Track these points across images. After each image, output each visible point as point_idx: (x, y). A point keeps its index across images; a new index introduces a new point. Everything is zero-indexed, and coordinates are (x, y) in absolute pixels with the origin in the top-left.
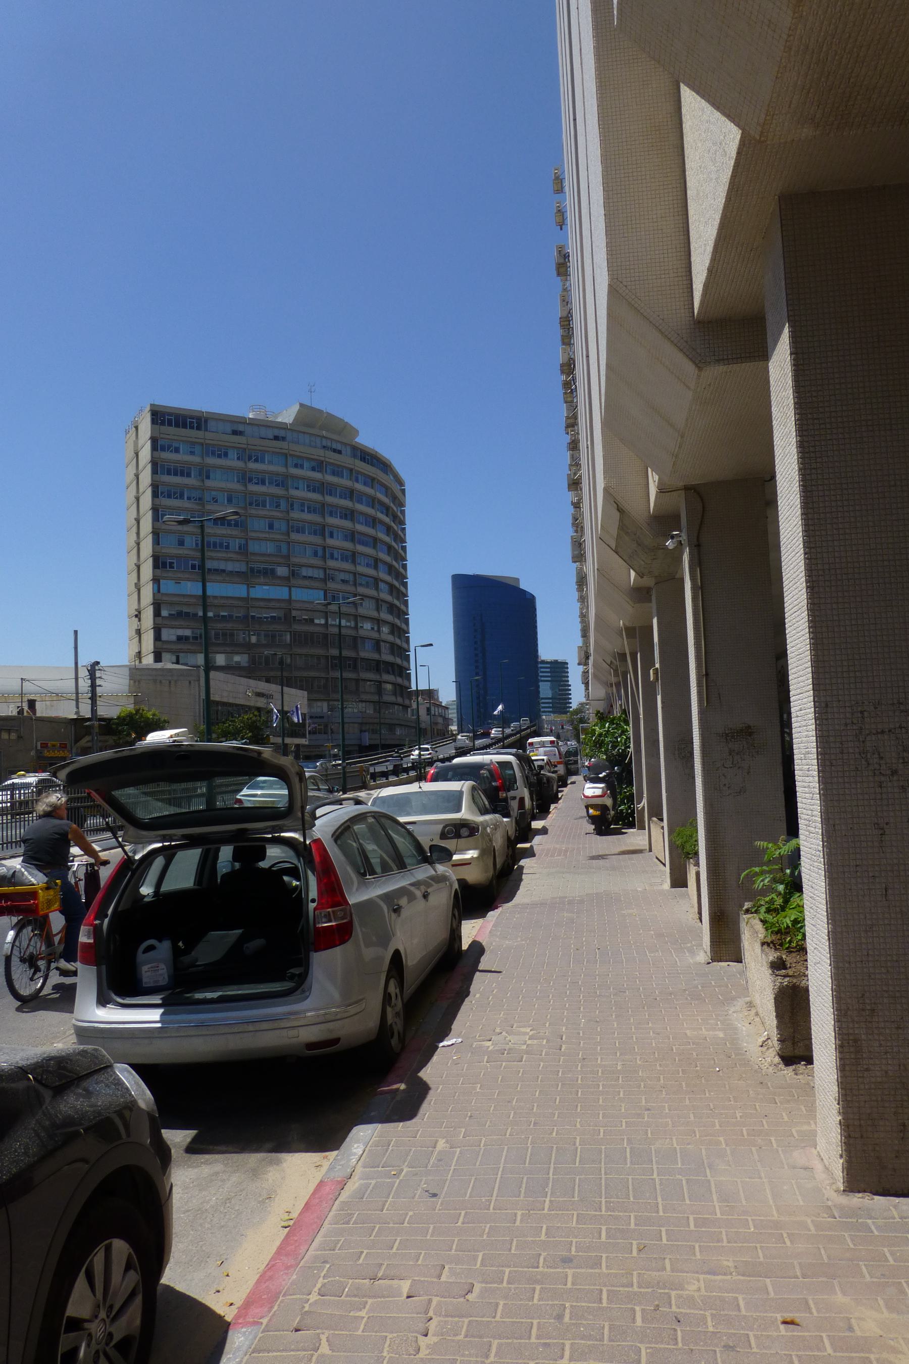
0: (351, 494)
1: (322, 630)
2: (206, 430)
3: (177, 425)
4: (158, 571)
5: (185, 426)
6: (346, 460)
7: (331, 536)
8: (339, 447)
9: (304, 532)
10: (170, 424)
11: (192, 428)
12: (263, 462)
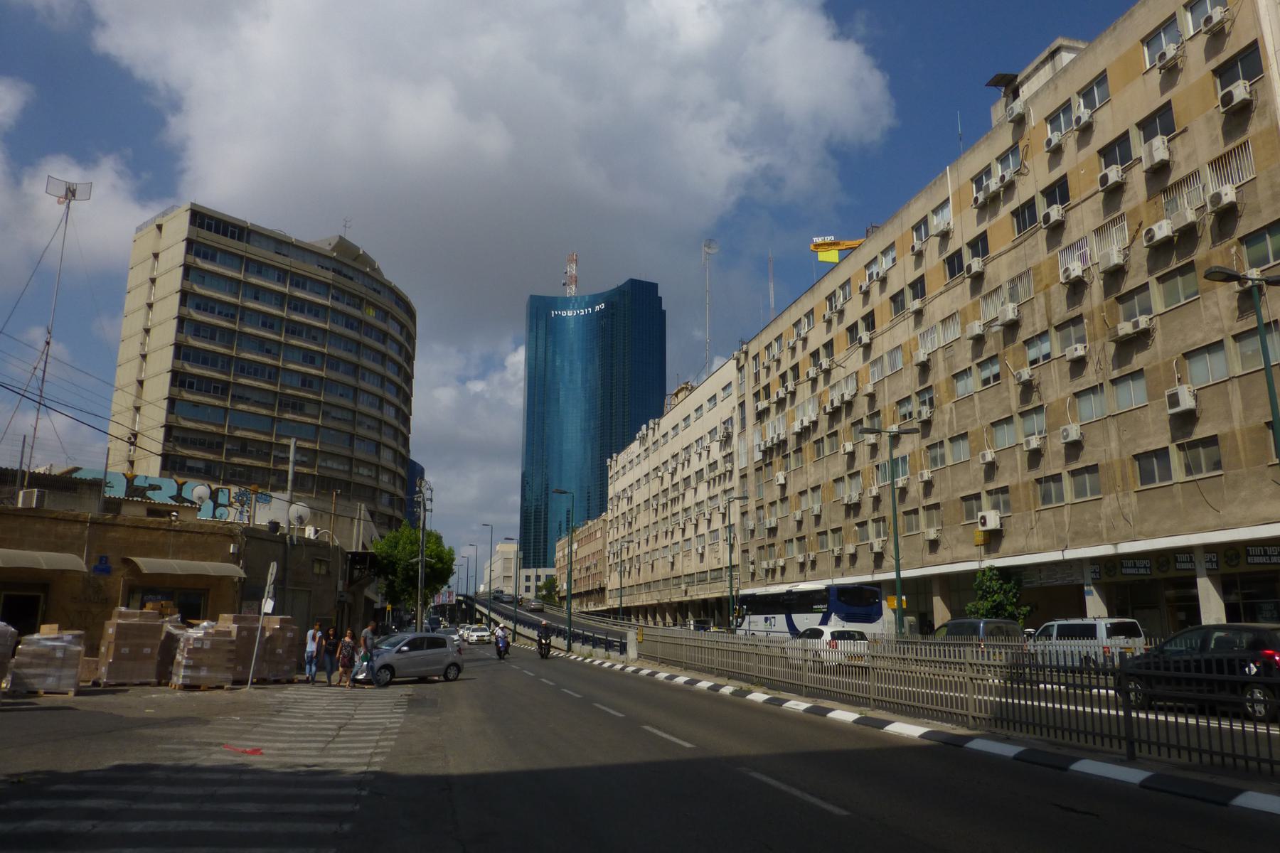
1: (344, 477)
2: (248, 242)
3: (217, 232)
4: (176, 390)
5: (225, 234)
6: (385, 301)
8: (379, 288)
9: (337, 370)
10: (209, 229)
11: (232, 237)
12: (304, 288)
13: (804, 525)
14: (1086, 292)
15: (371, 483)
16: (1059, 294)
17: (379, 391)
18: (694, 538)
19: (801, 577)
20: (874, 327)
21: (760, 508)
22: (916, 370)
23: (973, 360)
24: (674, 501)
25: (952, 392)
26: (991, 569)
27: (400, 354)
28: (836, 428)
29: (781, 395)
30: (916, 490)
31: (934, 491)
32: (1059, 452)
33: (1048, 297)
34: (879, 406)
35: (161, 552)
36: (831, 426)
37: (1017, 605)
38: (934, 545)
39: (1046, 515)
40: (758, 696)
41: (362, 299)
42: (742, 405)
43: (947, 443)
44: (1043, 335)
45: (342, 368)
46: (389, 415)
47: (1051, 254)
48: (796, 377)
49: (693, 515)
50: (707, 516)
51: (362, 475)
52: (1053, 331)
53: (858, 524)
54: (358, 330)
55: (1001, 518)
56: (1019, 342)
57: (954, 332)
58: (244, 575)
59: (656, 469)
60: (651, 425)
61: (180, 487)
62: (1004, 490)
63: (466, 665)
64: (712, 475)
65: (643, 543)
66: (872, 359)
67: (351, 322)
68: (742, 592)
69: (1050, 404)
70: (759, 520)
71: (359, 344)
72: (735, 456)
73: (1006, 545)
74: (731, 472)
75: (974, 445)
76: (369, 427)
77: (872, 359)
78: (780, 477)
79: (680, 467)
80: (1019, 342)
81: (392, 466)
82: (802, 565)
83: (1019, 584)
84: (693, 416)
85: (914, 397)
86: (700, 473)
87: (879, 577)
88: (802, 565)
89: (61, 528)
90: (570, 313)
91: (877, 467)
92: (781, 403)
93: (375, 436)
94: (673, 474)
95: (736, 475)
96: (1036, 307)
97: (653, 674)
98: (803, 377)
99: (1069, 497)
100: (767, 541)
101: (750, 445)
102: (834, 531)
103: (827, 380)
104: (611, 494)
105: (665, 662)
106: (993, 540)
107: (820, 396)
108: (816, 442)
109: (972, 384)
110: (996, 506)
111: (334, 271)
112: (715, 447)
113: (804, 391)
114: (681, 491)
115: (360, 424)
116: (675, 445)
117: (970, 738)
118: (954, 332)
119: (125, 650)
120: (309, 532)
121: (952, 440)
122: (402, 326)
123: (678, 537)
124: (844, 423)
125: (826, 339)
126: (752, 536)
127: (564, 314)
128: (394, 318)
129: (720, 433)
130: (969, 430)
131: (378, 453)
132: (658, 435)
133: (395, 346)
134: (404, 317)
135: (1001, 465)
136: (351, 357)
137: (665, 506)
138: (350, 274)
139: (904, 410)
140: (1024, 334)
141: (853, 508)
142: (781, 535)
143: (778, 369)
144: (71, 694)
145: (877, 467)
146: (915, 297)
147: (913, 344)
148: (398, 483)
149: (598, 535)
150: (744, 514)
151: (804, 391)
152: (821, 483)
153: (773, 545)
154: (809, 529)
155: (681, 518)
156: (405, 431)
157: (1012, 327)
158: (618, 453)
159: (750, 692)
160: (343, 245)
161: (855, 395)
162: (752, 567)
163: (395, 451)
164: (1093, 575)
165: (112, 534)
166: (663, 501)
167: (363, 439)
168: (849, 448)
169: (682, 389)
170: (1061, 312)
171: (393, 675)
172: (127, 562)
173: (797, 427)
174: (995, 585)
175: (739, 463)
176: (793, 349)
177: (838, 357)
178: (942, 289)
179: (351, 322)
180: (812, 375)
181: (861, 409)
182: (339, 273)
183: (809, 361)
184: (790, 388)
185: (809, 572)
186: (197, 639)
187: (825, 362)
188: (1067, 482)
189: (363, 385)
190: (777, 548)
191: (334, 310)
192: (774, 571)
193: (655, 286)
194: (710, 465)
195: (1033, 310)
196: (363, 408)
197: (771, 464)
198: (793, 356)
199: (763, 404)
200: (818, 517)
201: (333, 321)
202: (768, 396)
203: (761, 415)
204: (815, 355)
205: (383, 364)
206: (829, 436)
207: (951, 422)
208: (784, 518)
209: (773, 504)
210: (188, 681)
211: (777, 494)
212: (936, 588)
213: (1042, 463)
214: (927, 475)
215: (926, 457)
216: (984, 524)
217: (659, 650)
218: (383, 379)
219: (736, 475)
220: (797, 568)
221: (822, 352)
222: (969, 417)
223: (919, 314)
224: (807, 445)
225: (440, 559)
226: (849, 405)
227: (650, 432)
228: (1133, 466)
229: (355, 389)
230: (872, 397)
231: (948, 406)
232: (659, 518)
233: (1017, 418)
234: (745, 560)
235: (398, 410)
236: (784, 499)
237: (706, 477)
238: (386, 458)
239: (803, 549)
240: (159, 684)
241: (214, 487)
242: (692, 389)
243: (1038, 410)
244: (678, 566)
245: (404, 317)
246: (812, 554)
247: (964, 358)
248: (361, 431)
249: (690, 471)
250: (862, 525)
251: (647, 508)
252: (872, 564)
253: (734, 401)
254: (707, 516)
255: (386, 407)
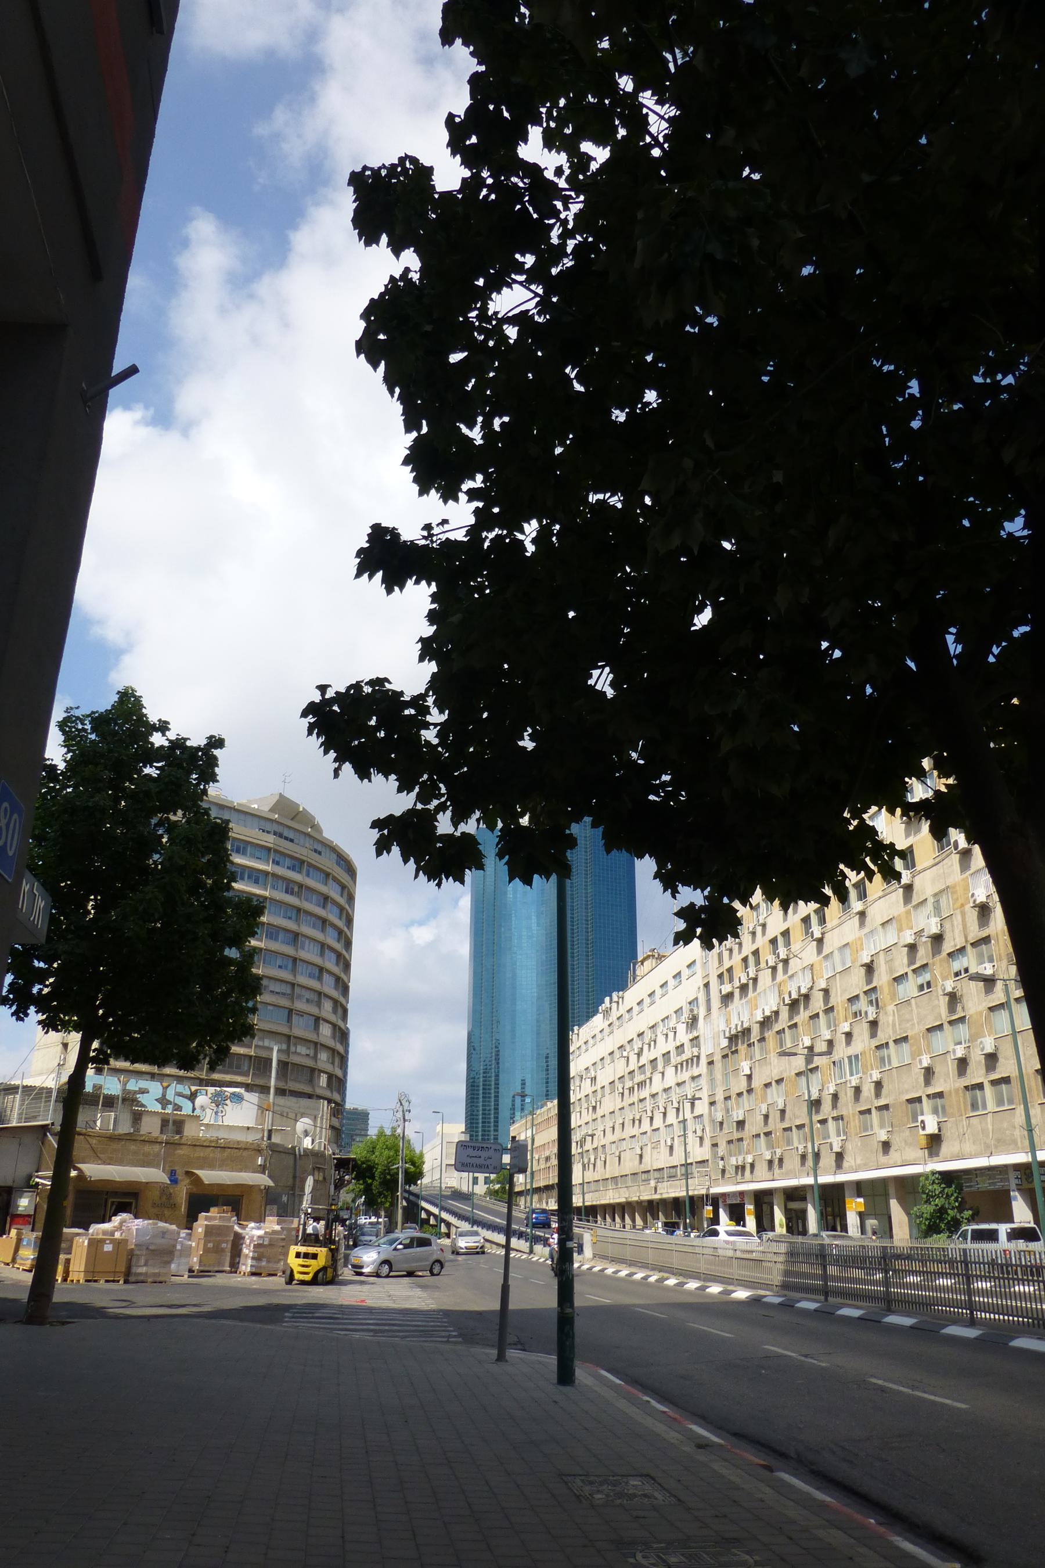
0: (326, 899)
6: (327, 862)
7: (303, 948)
8: (319, 848)
9: (276, 940)
12: (244, 853)
13: (770, 1120)
14: (992, 915)
15: (310, 1063)
16: (973, 915)
17: (318, 960)
18: (662, 1129)
19: (769, 1176)
20: (825, 922)
21: (727, 1098)
22: (863, 970)
23: (909, 966)
24: (641, 1085)
25: (894, 995)
26: (933, 1173)
27: (340, 919)
28: (796, 1020)
29: (744, 981)
30: (868, 1090)
31: (884, 1091)
32: (980, 1062)
33: (963, 914)
34: (833, 1002)
35: (223, 1165)
36: (791, 1018)
37: (961, 1209)
38: (886, 1146)
39: (975, 1121)
40: (672, 1282)
41: (302, 862)
42: (707, 985)
43: (891, 1044)
44: (962, 950)
45: (281, 936)
46: (328, 986)
47: (964, 876)
48: (758, 962)
49: (661, 1100)
50: (676, 1105)
51: (299, 1054)
52: (969, 947)
53: (820, 1122)
54: (298, 895)
55: (939, 1123)
56: (944, 954)
57: (889, 938)
58: (271, 1184)
59: (621, 1047)
60: (615, 998)
61: (165, 1088)
62: (940, 1095)
63: (447, 1264)
64: (679, 1059)
65: (609, 1131)
66: (824, 954)
67: (291, 887)
68: (713, 1191)
69: (971, 1016)
70: (728, 1111)
71: (299, 910)
72: (702, 1039)
73: (945, 1149)
74: (698, 1057)
75: (914, 1049)
76: (308, 1001)
77: (824, 954)
78: (745, 1067)
79: (646, 1047)
80: (944, 954)
81: (331, 1043)
82: (770, 1162)
83: (960, 1188)
84: (659, 992)
85: (862, 996)
86: (666, 1055)
87: (841, 1178)
88: (770, 1162)
89: (147, 1148)
91: (834, 1063)
92: (744, 988)
93: (313, 1010)
94: (639, 1055)
95: (703, 1061)
96: (955, 923)
97: (603, 1270)
98: (763, 965)
99: (991, 1106)
100: (736, 1135)
101: (716, 1030)
102: (800, 1127)
103: (785, 970)
104: (573, 1072)
105: (614, 1260)
106: (934, 1142)
107: (780, 985)
108: (778, 1032)
109: (909, 988)
110: (935, 1111)
111: (275, 834)
112: (682, 1028)
113: (765, 977)
114: (648, 1075)
115: (300, 997)
116: (640, 1023)
117: (765, 1296)
118: (889, 938)
119: (210, 1245)
120: (307, 1143)
121: (895, 1041)
122: (343, 887)
123: (646, 1126)
124: (802, 1016)
125: (783, 928)
126: (721, 1129)
128: (335, 879)
129: (685, 1015)
130: (910, 1033)
131: (316, 1027)
132: (623, 1009)
133: (336, 910)
134: (344, 877)
135: (936, 1070)
136: (291, 925)
137: (631, 1090)
138: (291, 835)
139: (855, 1008)
140: (948, 947)
141: (815, 1104)
142: (750, 1129)
143: (740, 952)
144: (186, 1276)
145: (834, 1063)
146: (860, 898)
147: (859, 943)
148: (337, 1061)
150: (712, 1104)
151: (765, 977)
152: (784, 1076)
153: (741, 1140)
154: (775, 1124)
155: (648, 1104)
156: (344, 1002)
157: (938, 939)
158: (580, 1026)
159: (667, 1279)
160: (283, 805)
161: (811, 988)
162: (721, 1163)
163: (334, 1026)
164: (1017, 1181)
165: (179, 1152)
166: (629, 1084)
167: (301, 1014)
168: (807, 1042)
169: (648, 957)
170: (975, 932)
171: (391, 1270)
172: (189, 1174)
173: (759, 1018)
174: (937, 1189)
175: (707, 1048)
176: (754, 934)
177: (795, 947)
178: (881, 894)
179: (291, 887)
180: (771, 963)
181: (817, 1003)
182: (281, 836)
183: (768, 948)
184: (752, 975)
185: (777, 1171)
186: (259, 1237)
187: (783, 953)
188: (988, 1089)
189: (303, 954)
190: (745, 1143)
191: (274, 875)
192: (743, 1167)
194: (677, 1048)
195: (953, 926)
196: (302, 980)
197: (736, 1051)
198: (753, 941)
199: (727, 988)
200: (783, 1112)
201: (273, 887)
202: (731, 980)
203: (727, 998)
204: (774, 941)
205: (323, 931)
206: (790, 1027)
207: (894, 1025)
208: (751, 1110)
209: (740, 1095)
210: (254, 1270)
211: (743, 1085)
212: (892, 1191)
213: (968, 1071)
214: (876, 1076)
215: (875, 1056)
216: (924, 1128)
217: (610, 1250)
218: (323, 946)
219: (703, 1061)
220: (765, 1165)
221: (780, 941)
222: (908, 1021)
223: (862, 914)
224: (769, 1035)
225: (413, 1163)
226: (807, 997)
227: (614, 1005)
228: (1036, 1079)
229: (295, 960)
230: (826, 991)
231: (891, 1008)
232: (625, 1104)
233: (946, 1026)
234: (715, 1155)
235: (338, 979)
236: (750, 1091)
237: (675, 1059)
238: (326, 1030)
239: (770, 1146)
240: (231, 1272)
241: (193, 1088)
242: (661, 958)
243: (962, 1019)
244: (646, 1159)
245: (344, 877)
246: (779, 1152)
247: (902, 965)
248: (299, 1005)
249: (657, 1053)
250: (823, 1122)
251: (612, 1091)
252: (834, 1164)
253: (698, 981)
254: (676, 1105)
255: (326, 976)
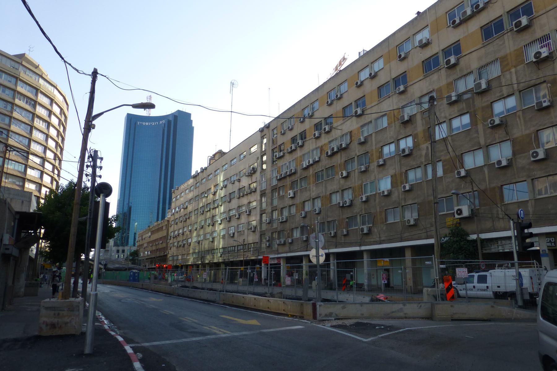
90: (147, 124)
127: (144, 124)
149: (164, 228)
151: (310, 145)
152: (321, 195)
181: (356, 150)
193: (189, 115)
